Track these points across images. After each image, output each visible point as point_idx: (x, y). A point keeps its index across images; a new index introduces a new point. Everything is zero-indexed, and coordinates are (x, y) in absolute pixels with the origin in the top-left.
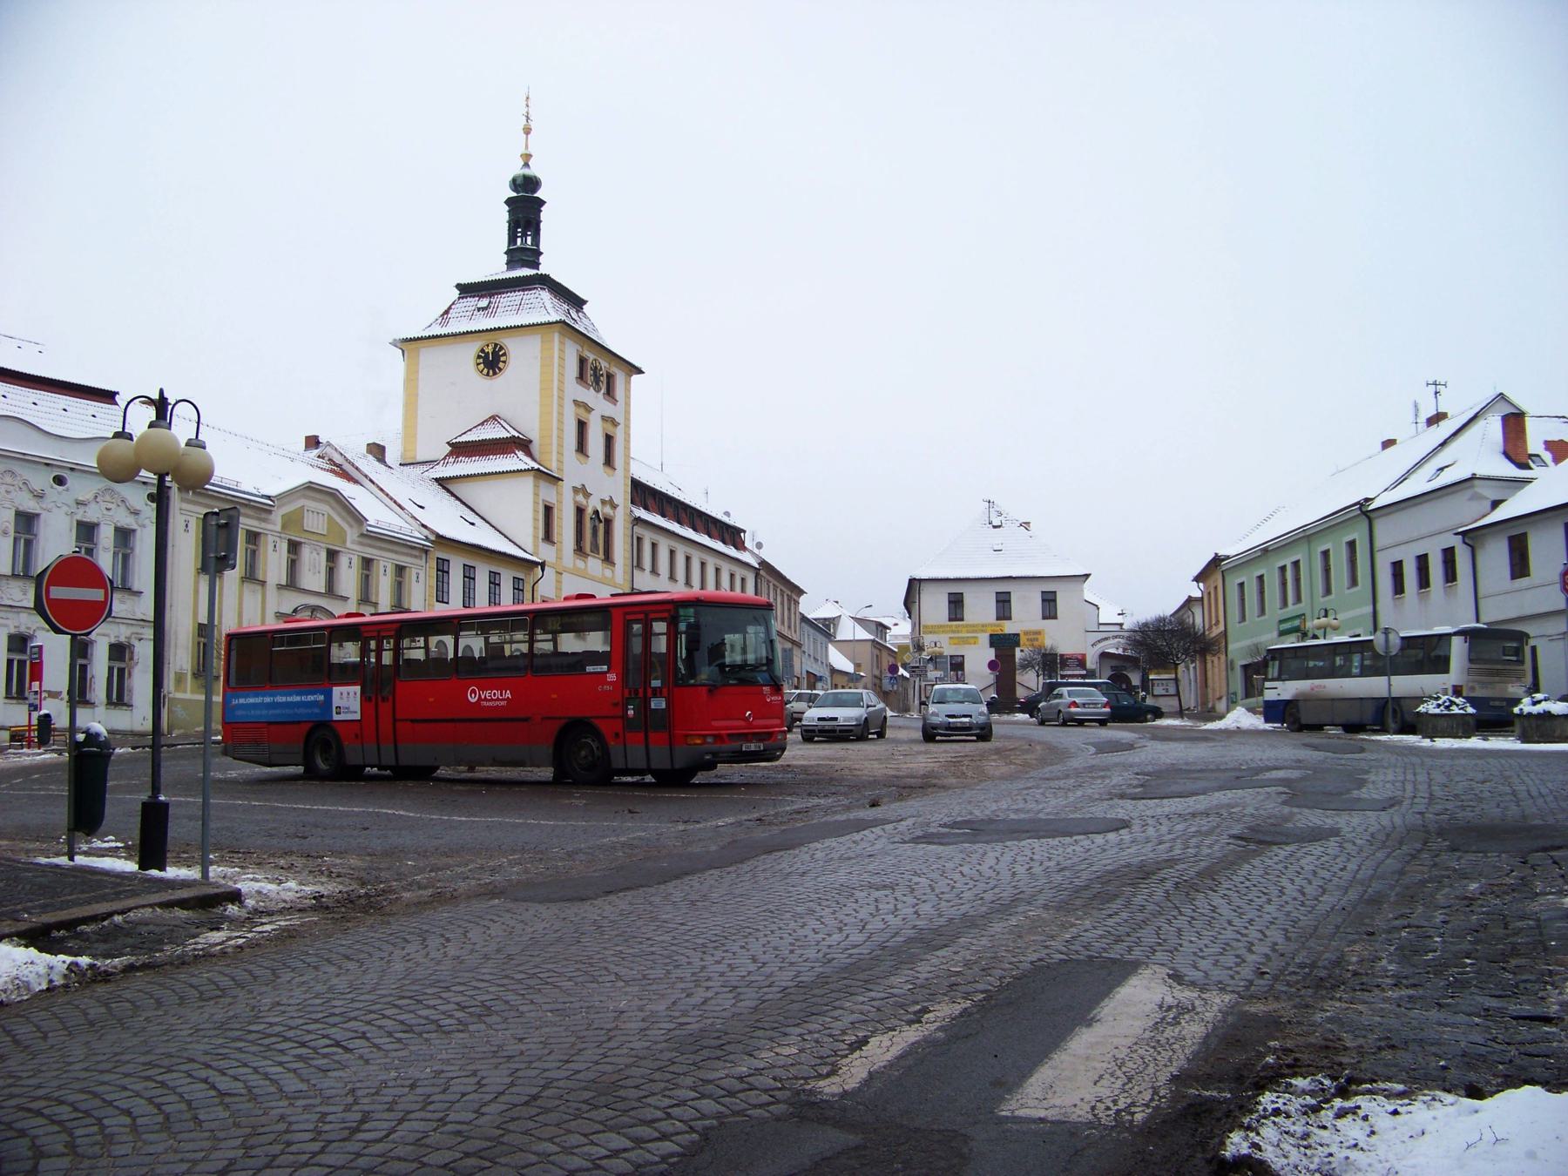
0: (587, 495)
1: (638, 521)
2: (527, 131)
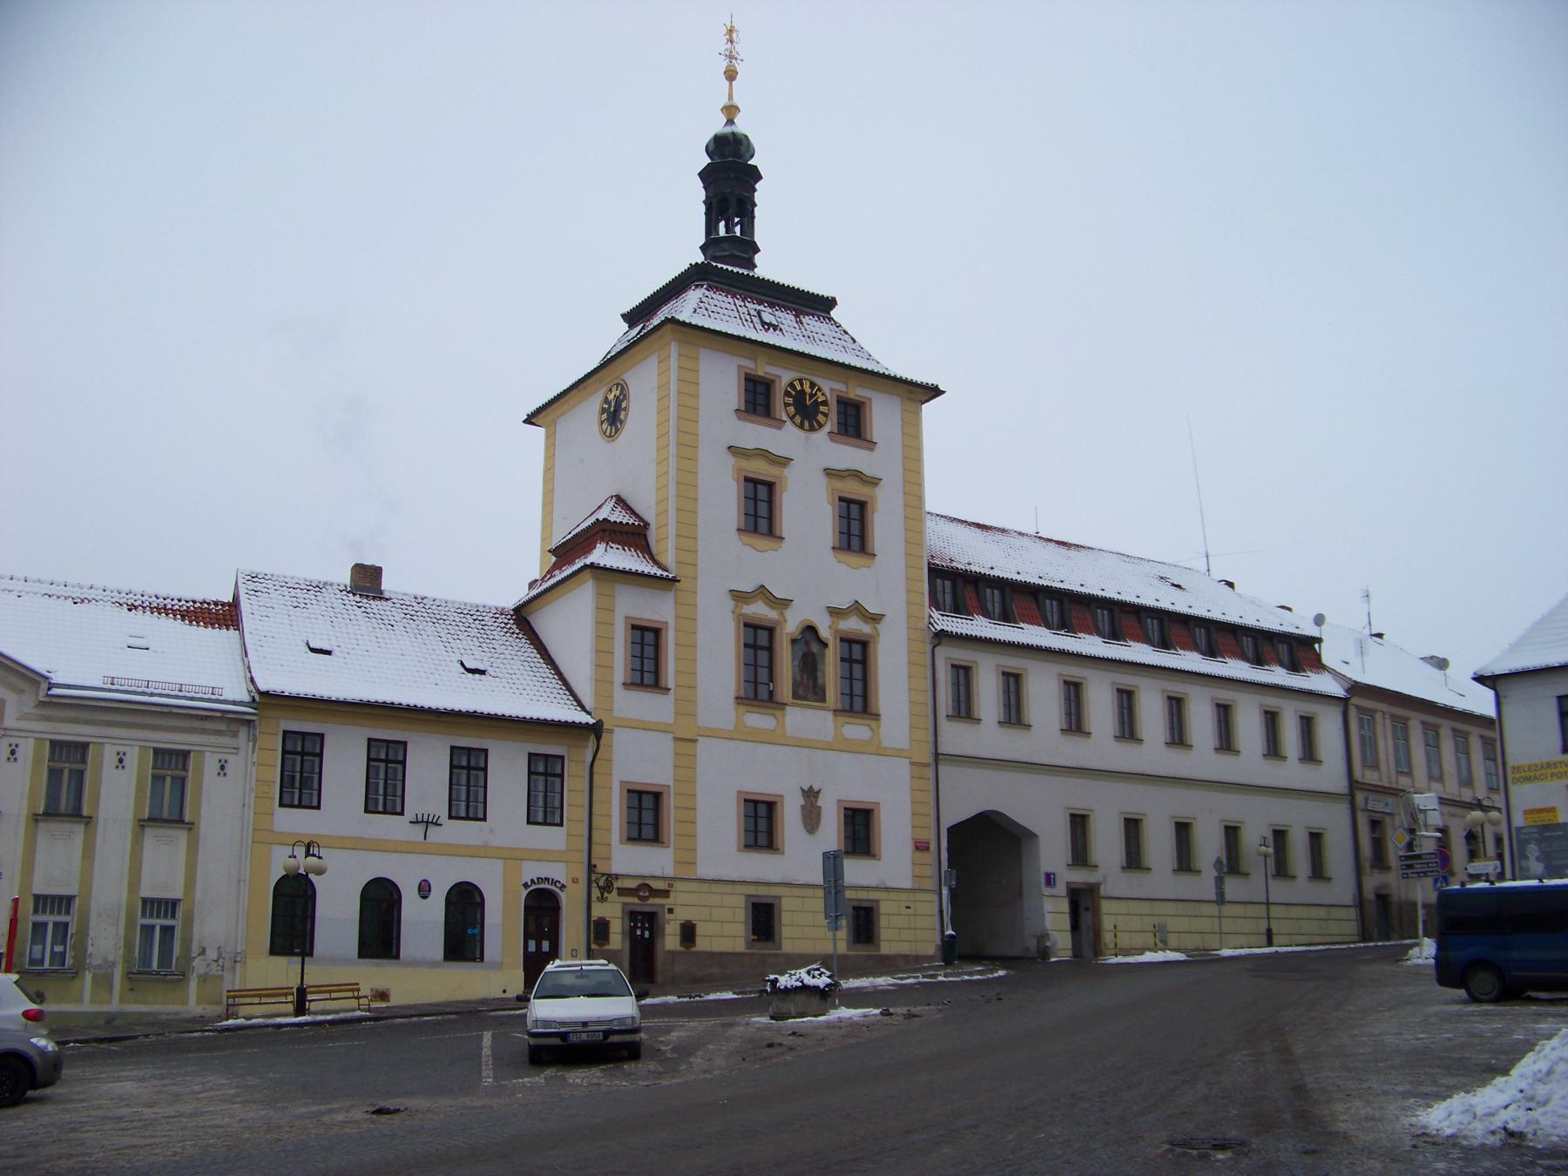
0: (785, 603)
1: (942, 636)
2: (731, 75)
